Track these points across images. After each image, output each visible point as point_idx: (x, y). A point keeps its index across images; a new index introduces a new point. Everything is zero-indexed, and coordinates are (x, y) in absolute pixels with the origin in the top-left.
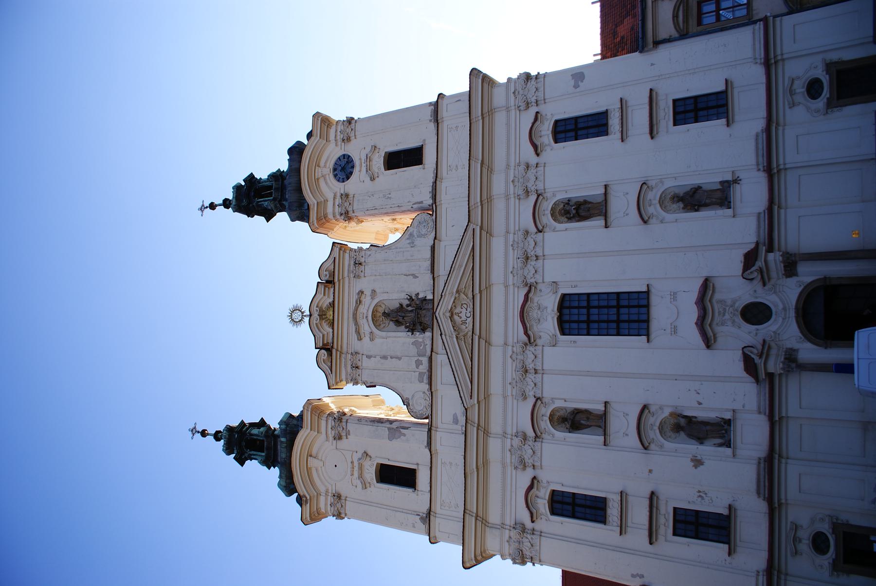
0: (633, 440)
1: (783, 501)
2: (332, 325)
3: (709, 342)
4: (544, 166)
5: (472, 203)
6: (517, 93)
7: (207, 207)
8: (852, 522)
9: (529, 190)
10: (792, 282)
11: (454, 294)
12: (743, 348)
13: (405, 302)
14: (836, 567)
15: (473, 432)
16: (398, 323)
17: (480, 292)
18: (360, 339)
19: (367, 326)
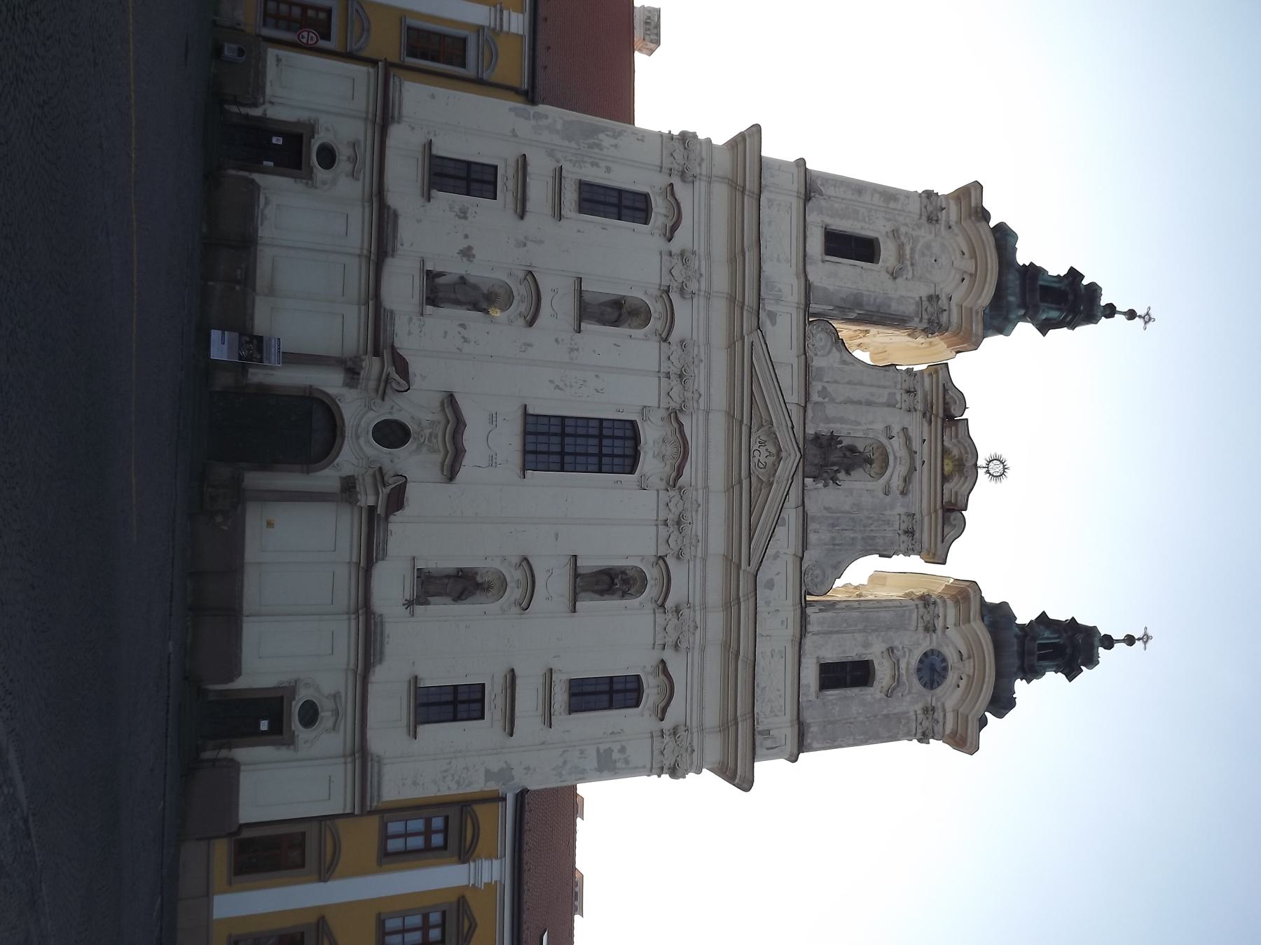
1: (367, 204)
2: (945, 451)
3: (450, 400)
4: (654, 644)
5: (752, 601)
6: (689, 749)
7: (1139, 639)
8: (292, 180)
9: (675, 613)
10: (347, 470)
11: (775, 481)
12: (409, 389)
13: (842, 475)
14: (311, 128)
15: (750, 298)
16: (852, 449)
17: (740, 482)
18: (904, 430)
19: (896, 446)
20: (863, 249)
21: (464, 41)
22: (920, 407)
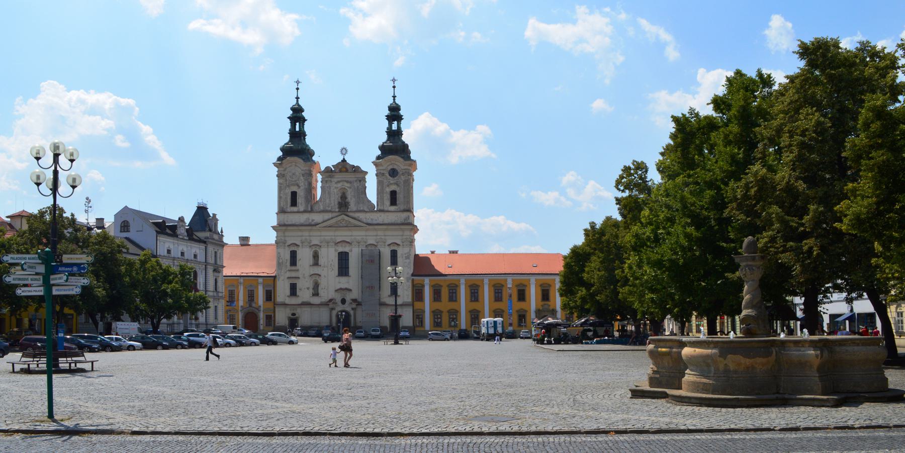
0: (312, 273)
3: (336, 291)
10: (351, 309)
16: (341, 198)
20: (294, 195)
21: (266, 290)
22: (330, 179)
